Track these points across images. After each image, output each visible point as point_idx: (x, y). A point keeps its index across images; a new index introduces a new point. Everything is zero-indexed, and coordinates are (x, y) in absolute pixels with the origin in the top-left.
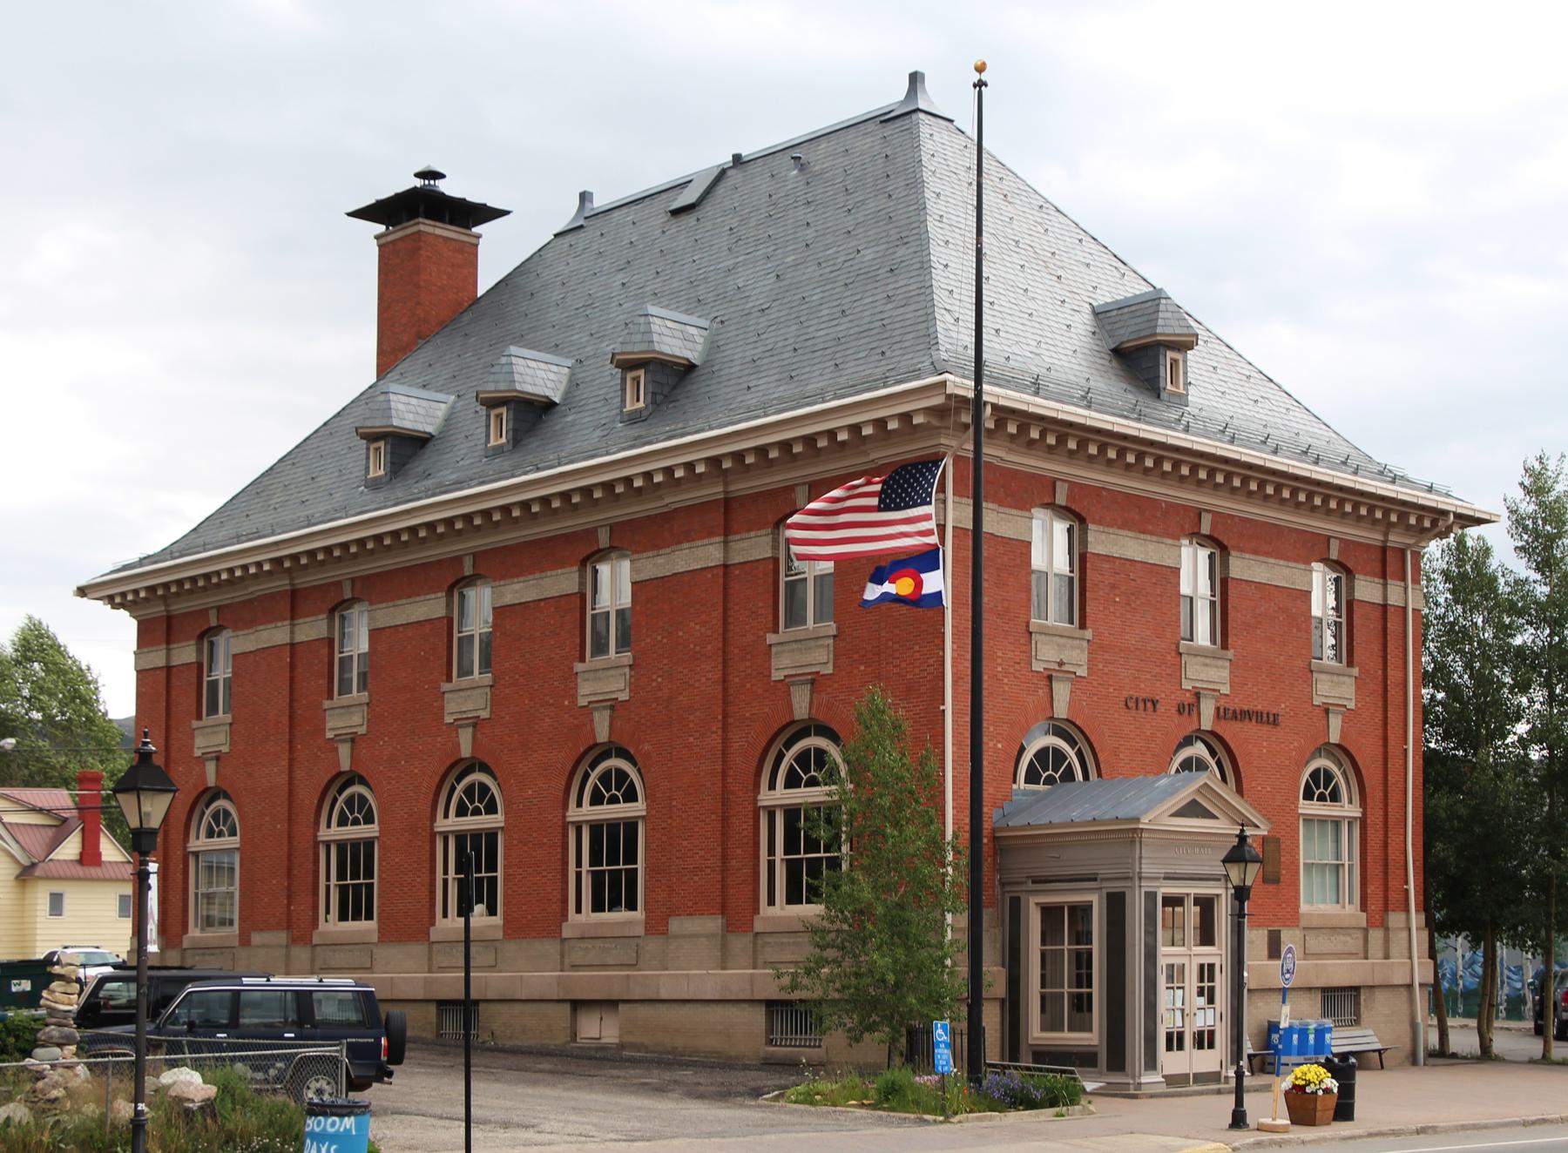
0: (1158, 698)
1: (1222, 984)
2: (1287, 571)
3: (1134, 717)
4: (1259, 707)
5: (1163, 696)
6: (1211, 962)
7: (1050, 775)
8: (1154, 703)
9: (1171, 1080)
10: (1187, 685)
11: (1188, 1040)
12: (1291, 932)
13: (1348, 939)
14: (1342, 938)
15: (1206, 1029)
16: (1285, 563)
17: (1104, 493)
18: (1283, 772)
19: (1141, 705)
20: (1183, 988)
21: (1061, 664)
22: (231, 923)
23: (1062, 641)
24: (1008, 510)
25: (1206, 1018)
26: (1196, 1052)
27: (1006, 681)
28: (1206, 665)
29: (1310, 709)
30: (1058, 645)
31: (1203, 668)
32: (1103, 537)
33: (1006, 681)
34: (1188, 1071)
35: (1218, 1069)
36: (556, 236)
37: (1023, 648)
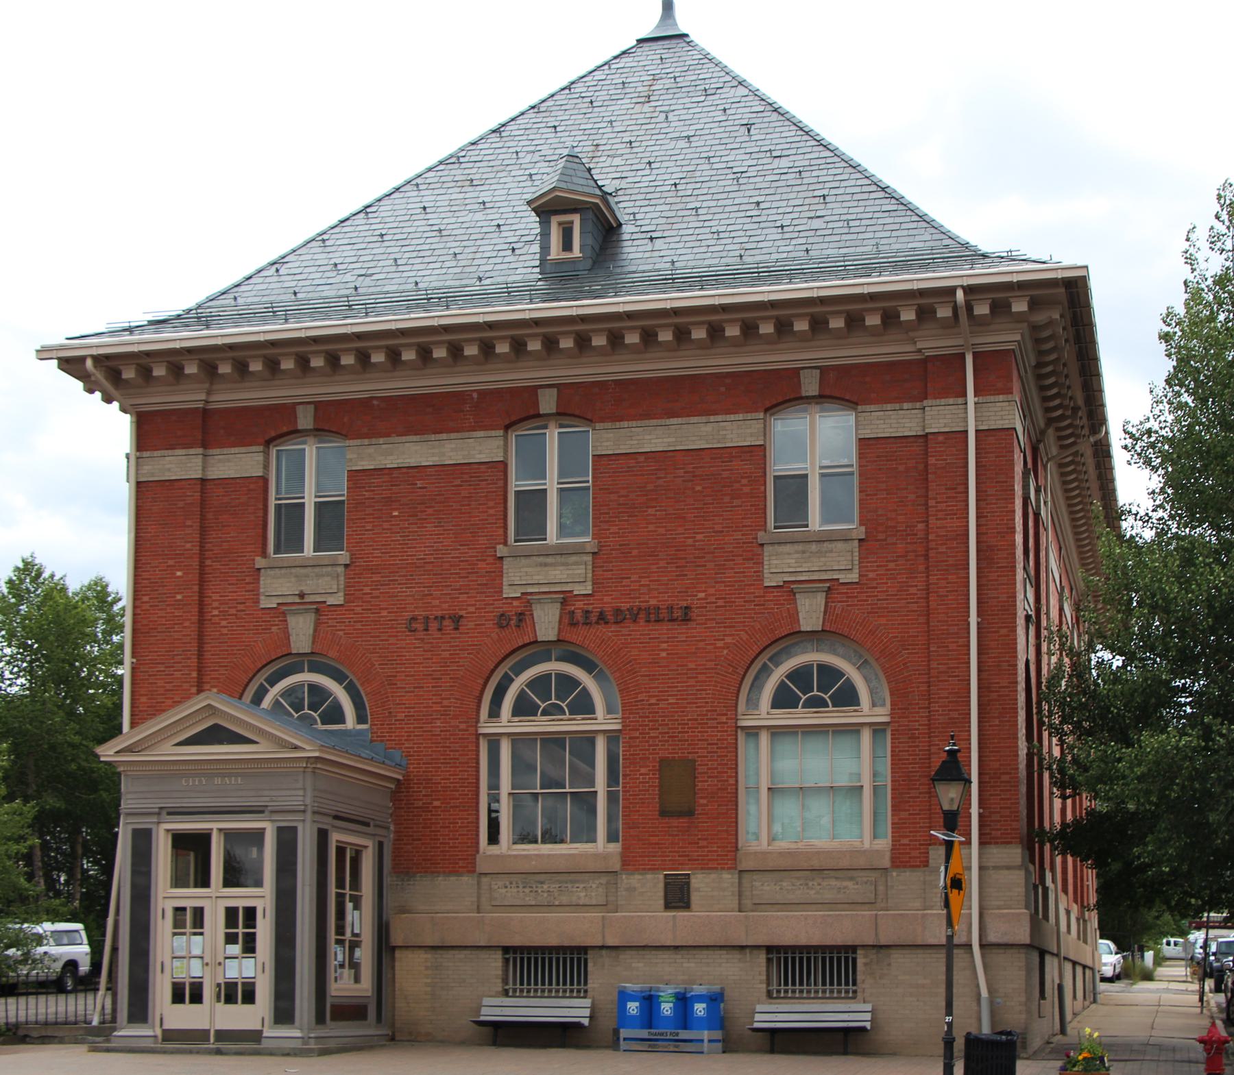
0: (462, 613)
1: (264, 930)
2: (709, 428)
3: (422, 640)
4: (653, 602)
5: (472, 609)
6: (198, 903)
7: (543, 702)
8: (457, 620)
9: (171, 1036)
10: (508, 592)
11: (208, 993)
12: (713, 876)
13: (849, 884)
14: (833, 882)
15: (188, 981)
16: (704, 419)
17: (375, 402)
18: (701, 678)
19: (434, 625)
20: (201, 934)
21: (302, 595)
22: (249, 997)
23: (303, 571)
24: (225, 451)
25: (241, 968)
26: (221, 1006)
27: (224, 623)
28: (546, 565)
29: (761, 592)
30: (296, 576)
31: (539, 569)
32: (371, 450)
33: (224, 623)
34: (207, 1027)
35: (259, 1027)
36: (640, 41)
37: (250, 587)
